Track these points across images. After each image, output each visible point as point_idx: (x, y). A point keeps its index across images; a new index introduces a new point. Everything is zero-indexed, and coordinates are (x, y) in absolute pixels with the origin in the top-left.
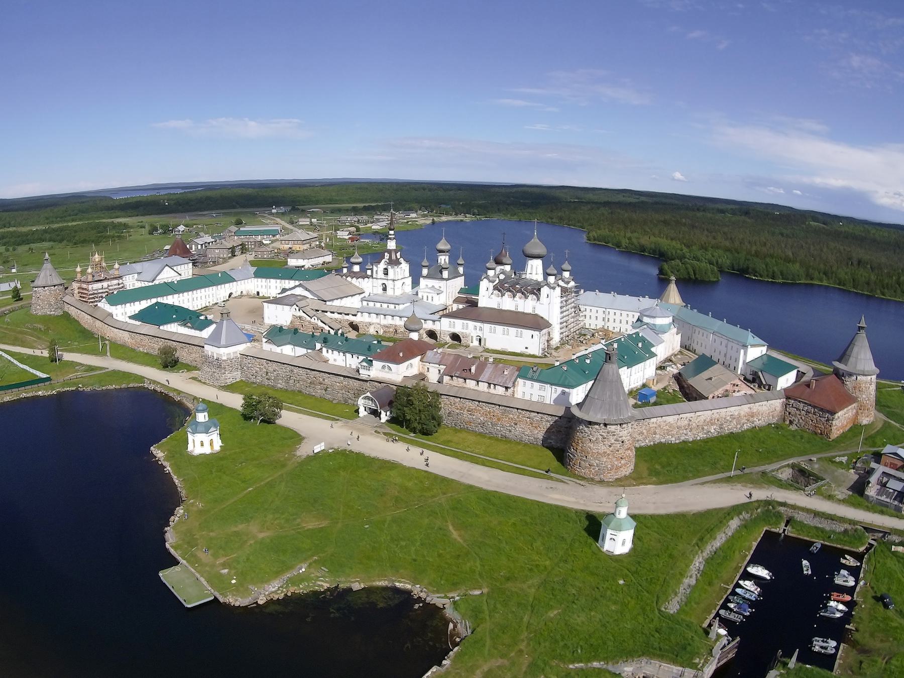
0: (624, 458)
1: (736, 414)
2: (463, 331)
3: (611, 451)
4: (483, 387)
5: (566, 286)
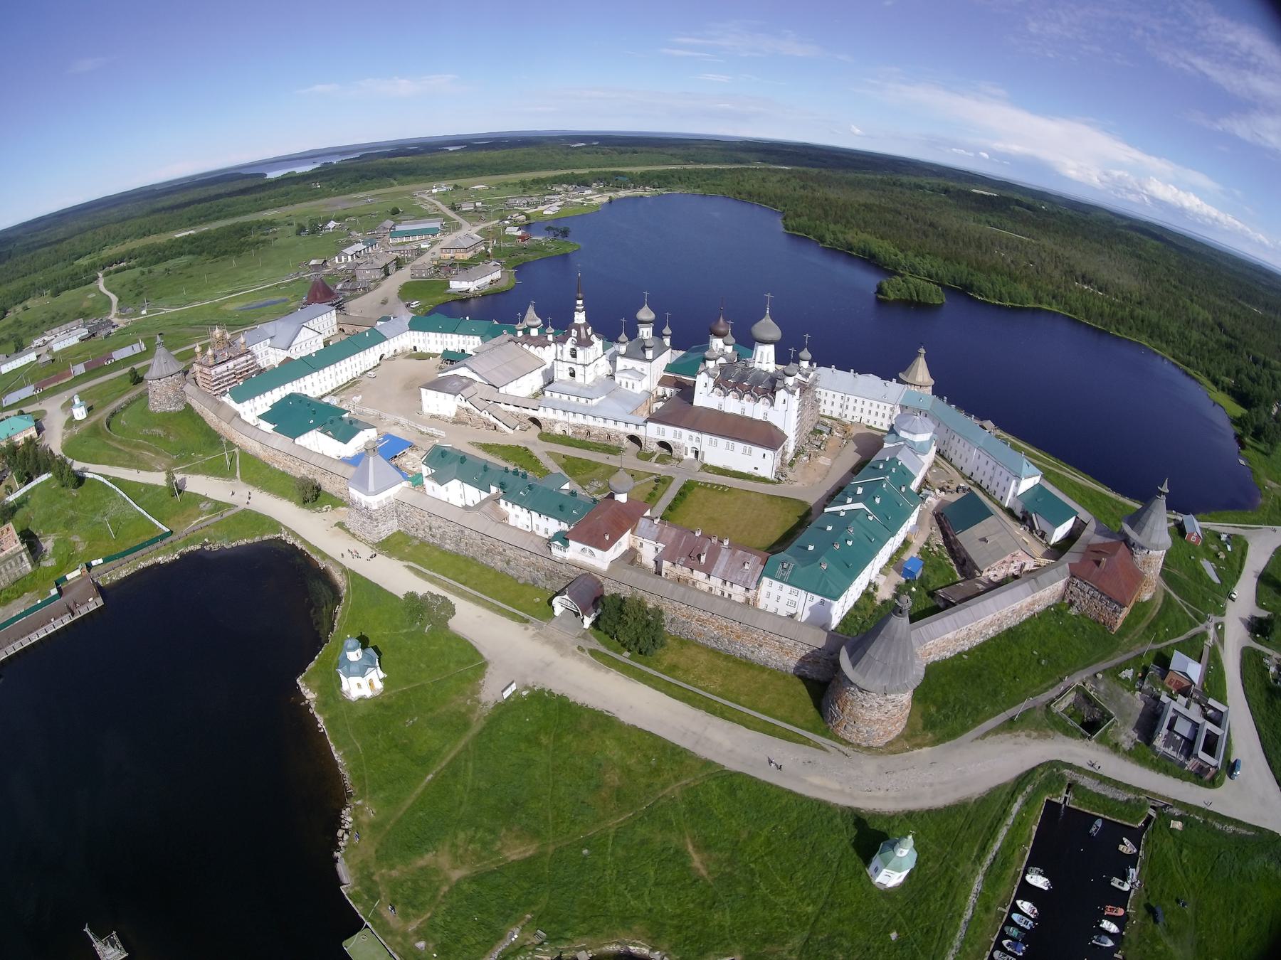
2: (674, 440)
4: (716, 582)
5: (804, 380)
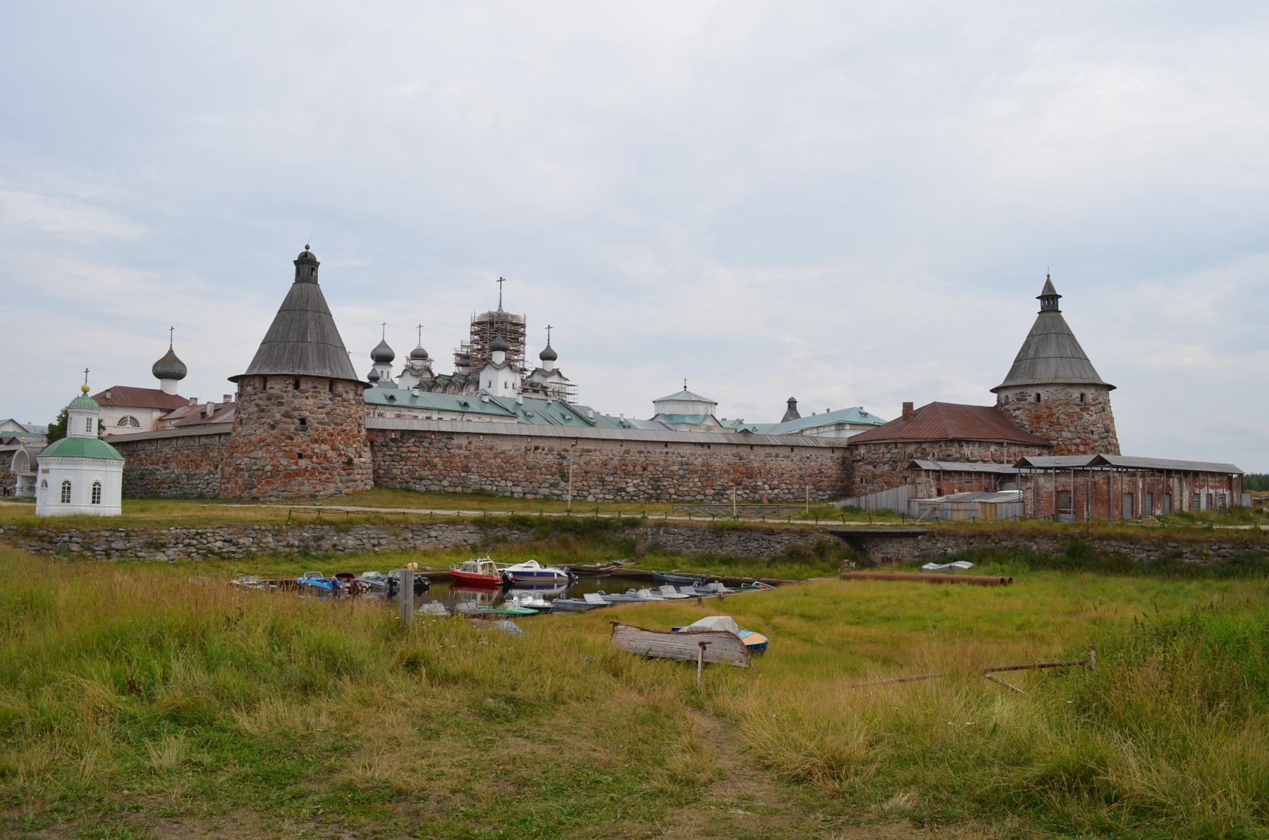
0: (305, 456)
3: (275, 437)
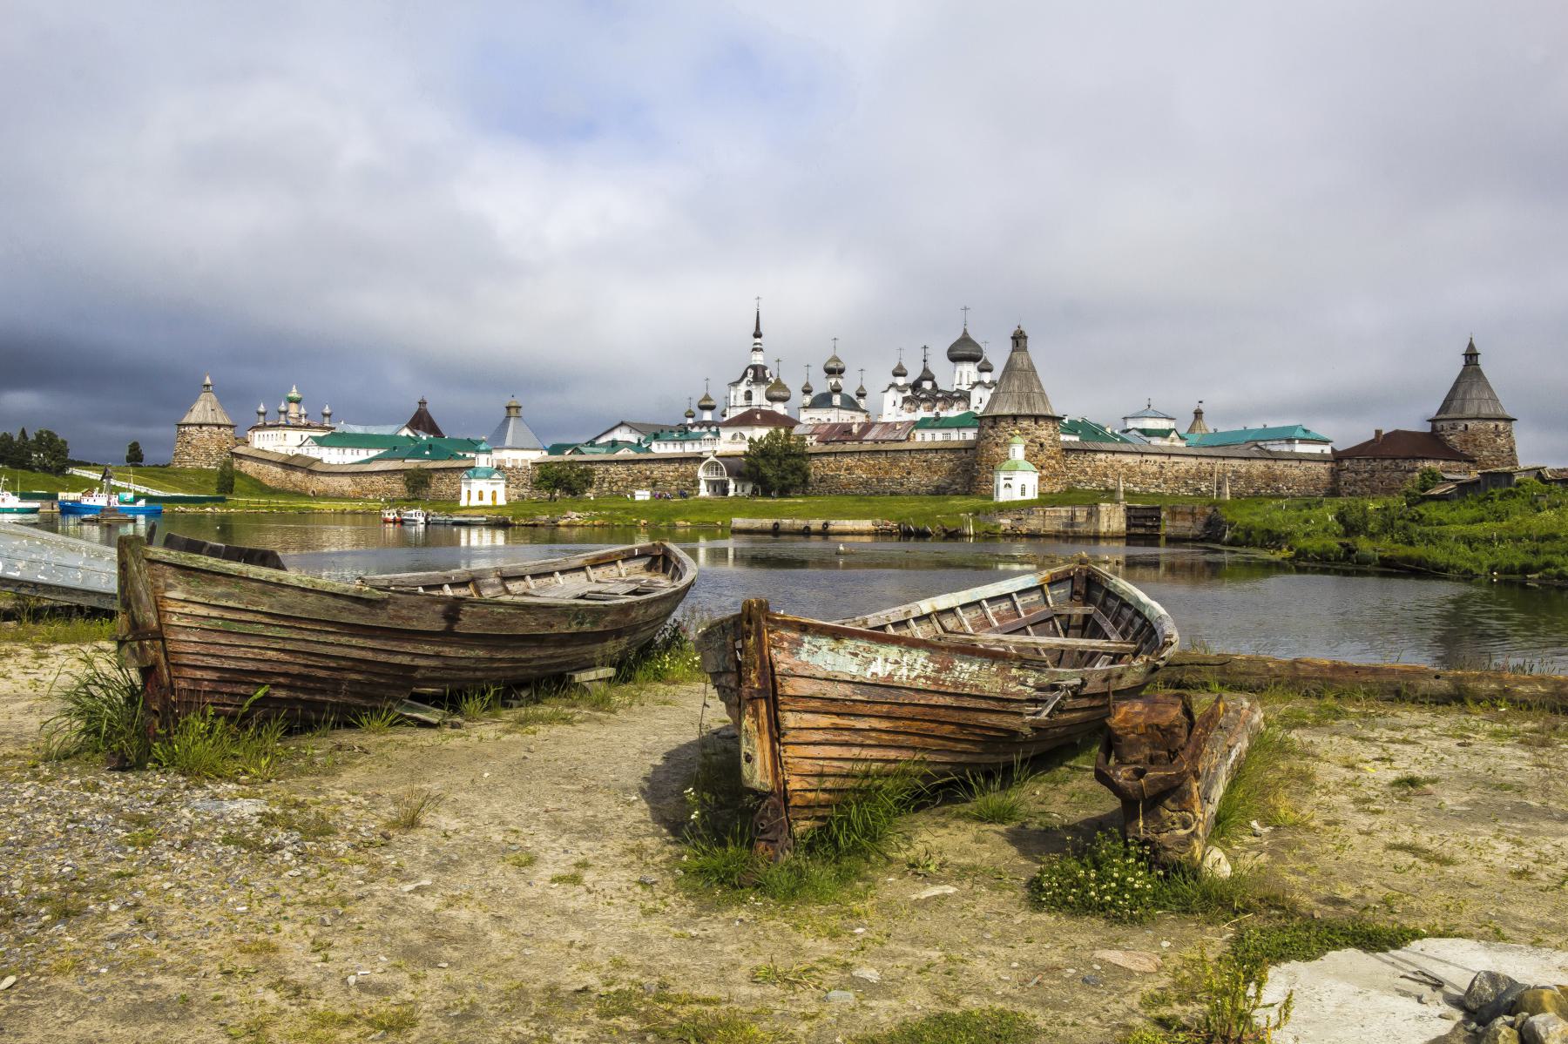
1: (1243, 470)
